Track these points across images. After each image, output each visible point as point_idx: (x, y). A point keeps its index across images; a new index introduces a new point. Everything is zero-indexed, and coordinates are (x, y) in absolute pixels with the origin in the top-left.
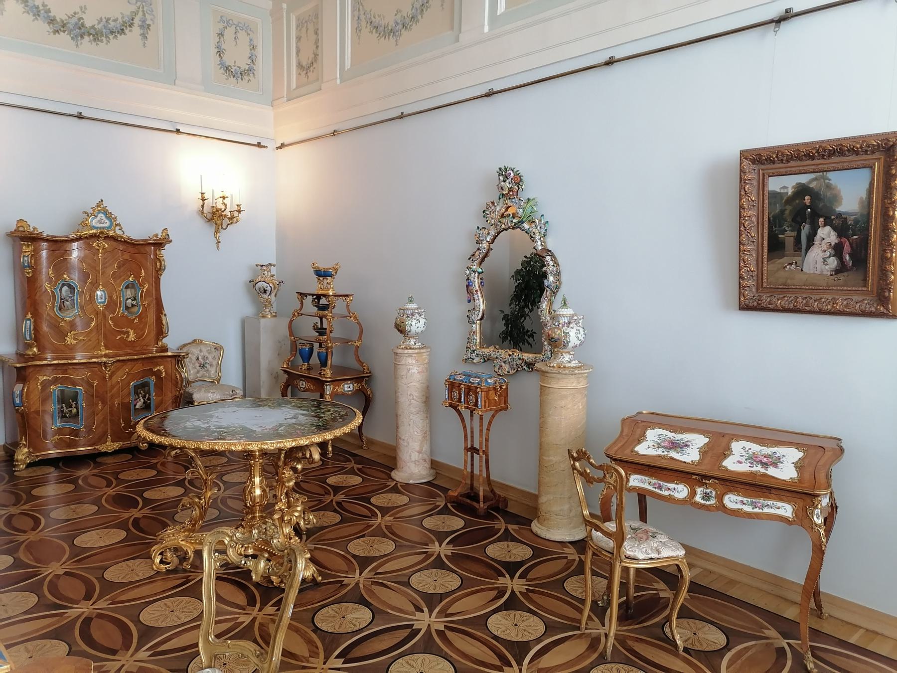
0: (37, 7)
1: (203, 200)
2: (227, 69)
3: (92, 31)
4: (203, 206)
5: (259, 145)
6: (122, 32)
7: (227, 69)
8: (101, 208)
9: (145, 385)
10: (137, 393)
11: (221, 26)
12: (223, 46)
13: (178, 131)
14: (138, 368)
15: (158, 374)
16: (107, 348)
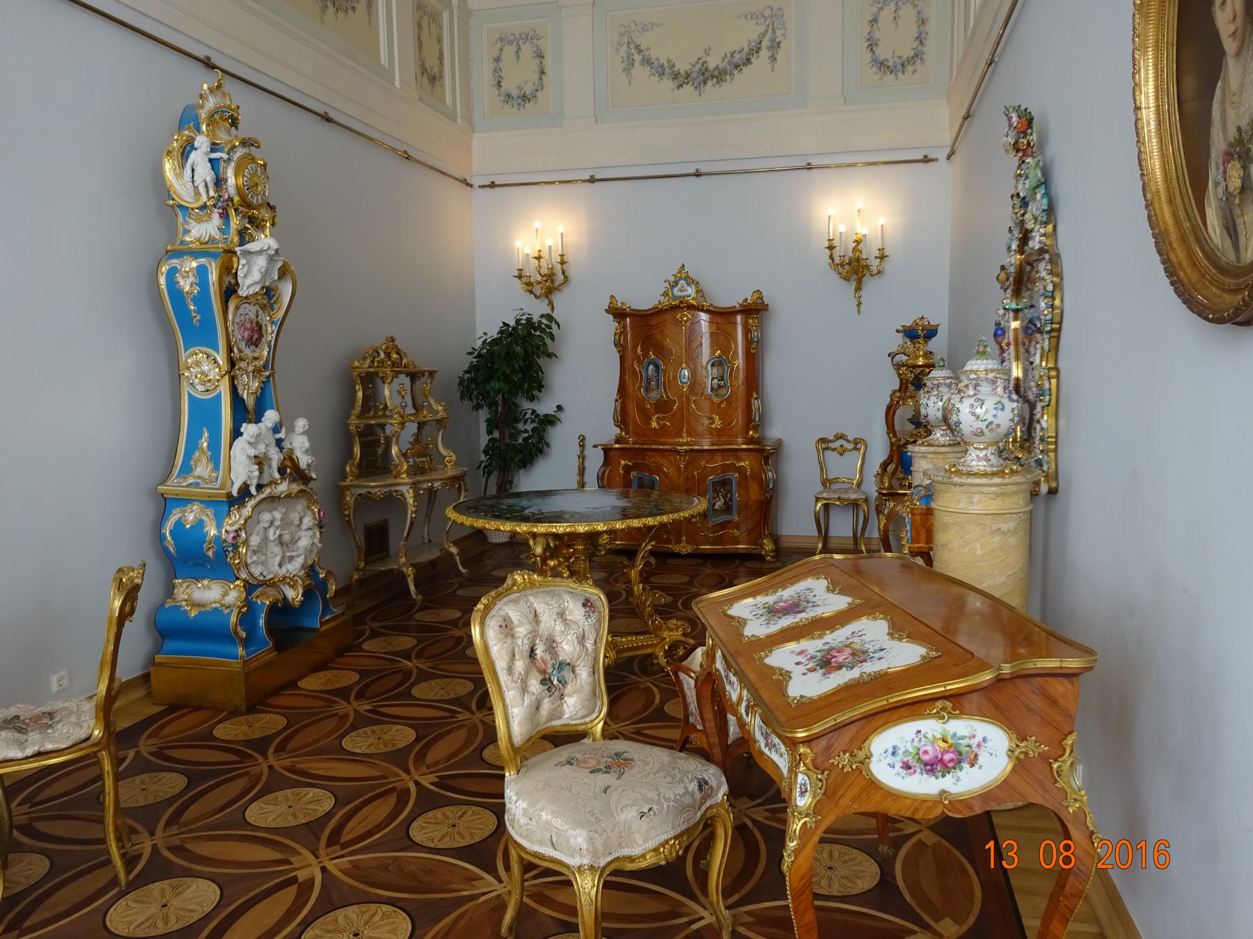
0: (662, 66)
1: (831, 248)
2: (882, 65)
3: (716, 73)
4: (831, 257)
5: (926, 160)
6: (748, 61)
7: (882, 65)
8: (683, 276)
9: (725, 483)
10: (716, 491)
11: (874, 9)
12: (877, 35)
13: (809, 167)
14: (718, 462)
15: (740, 470)
16: (689, 435)
